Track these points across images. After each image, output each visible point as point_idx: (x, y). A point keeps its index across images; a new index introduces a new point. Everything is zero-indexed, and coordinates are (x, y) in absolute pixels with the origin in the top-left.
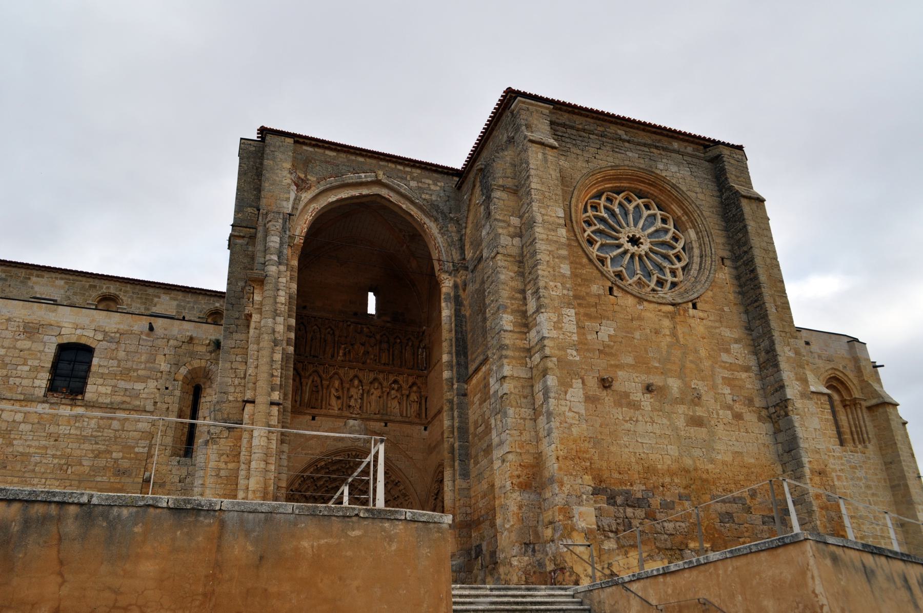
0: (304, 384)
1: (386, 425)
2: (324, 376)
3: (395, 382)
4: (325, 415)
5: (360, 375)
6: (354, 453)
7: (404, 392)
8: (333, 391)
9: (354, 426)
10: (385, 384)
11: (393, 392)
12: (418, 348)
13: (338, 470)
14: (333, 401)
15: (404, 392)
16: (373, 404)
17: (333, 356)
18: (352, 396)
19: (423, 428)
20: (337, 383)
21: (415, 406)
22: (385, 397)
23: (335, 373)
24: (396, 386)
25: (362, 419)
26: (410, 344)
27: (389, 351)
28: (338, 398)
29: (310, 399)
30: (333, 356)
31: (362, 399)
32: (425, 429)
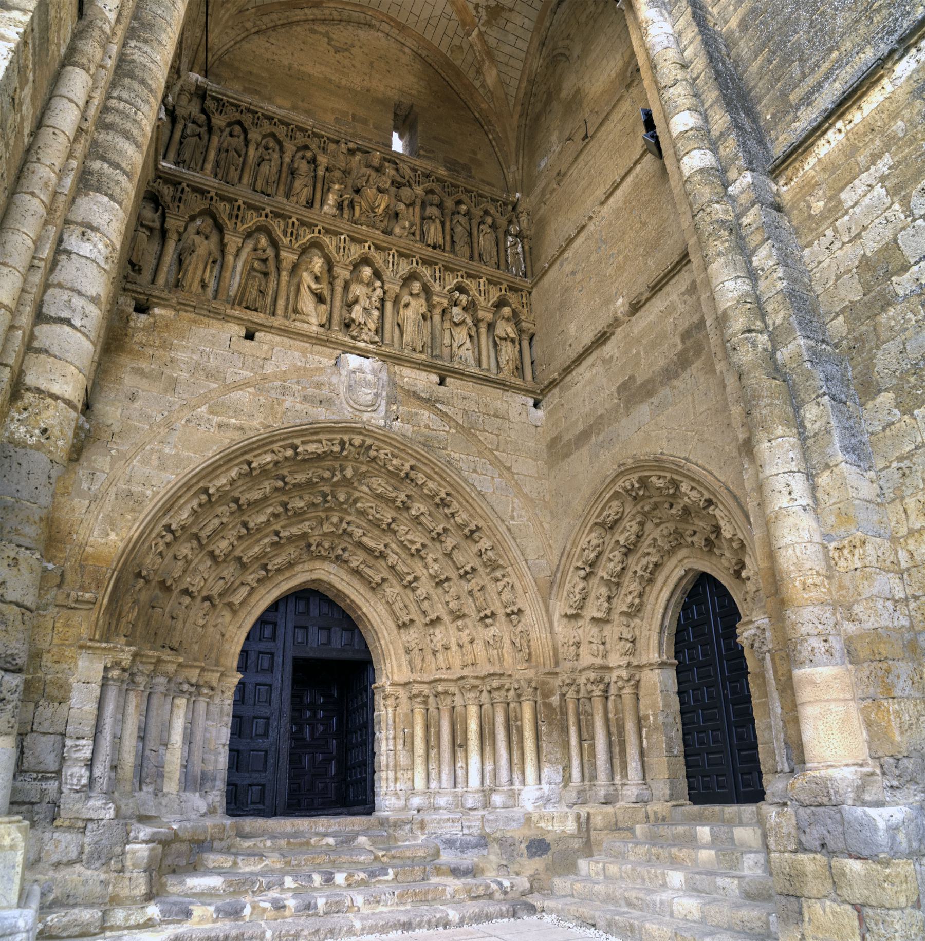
0: (231, 249)
1: (442, 382)
2: (286, 241)
3: (461, 289)
4: (284, 332)
5: (378, 258)
6: (357, 440)
7: (481, 314)
8: (307, 278)
9: (361, 370)
10: (436, 287)
11: (456, 310)
12: (507, 233)
13: (310, 484)
14: (307, 303)
15: (481, 314)
16: (409, 328)
17: (310, 204)
18: (356, 301)
19: (531, 402)
20: (318, 264)
21: (508, 352)
22: (437, 318)
23: (316, 244)
24: (464, 299)
25: (385, 358)
27: (443, 224)
28: (320, 299)
29: (243, 289)
30: (310, 204)
31: (382, 309)
32: (536, 405)
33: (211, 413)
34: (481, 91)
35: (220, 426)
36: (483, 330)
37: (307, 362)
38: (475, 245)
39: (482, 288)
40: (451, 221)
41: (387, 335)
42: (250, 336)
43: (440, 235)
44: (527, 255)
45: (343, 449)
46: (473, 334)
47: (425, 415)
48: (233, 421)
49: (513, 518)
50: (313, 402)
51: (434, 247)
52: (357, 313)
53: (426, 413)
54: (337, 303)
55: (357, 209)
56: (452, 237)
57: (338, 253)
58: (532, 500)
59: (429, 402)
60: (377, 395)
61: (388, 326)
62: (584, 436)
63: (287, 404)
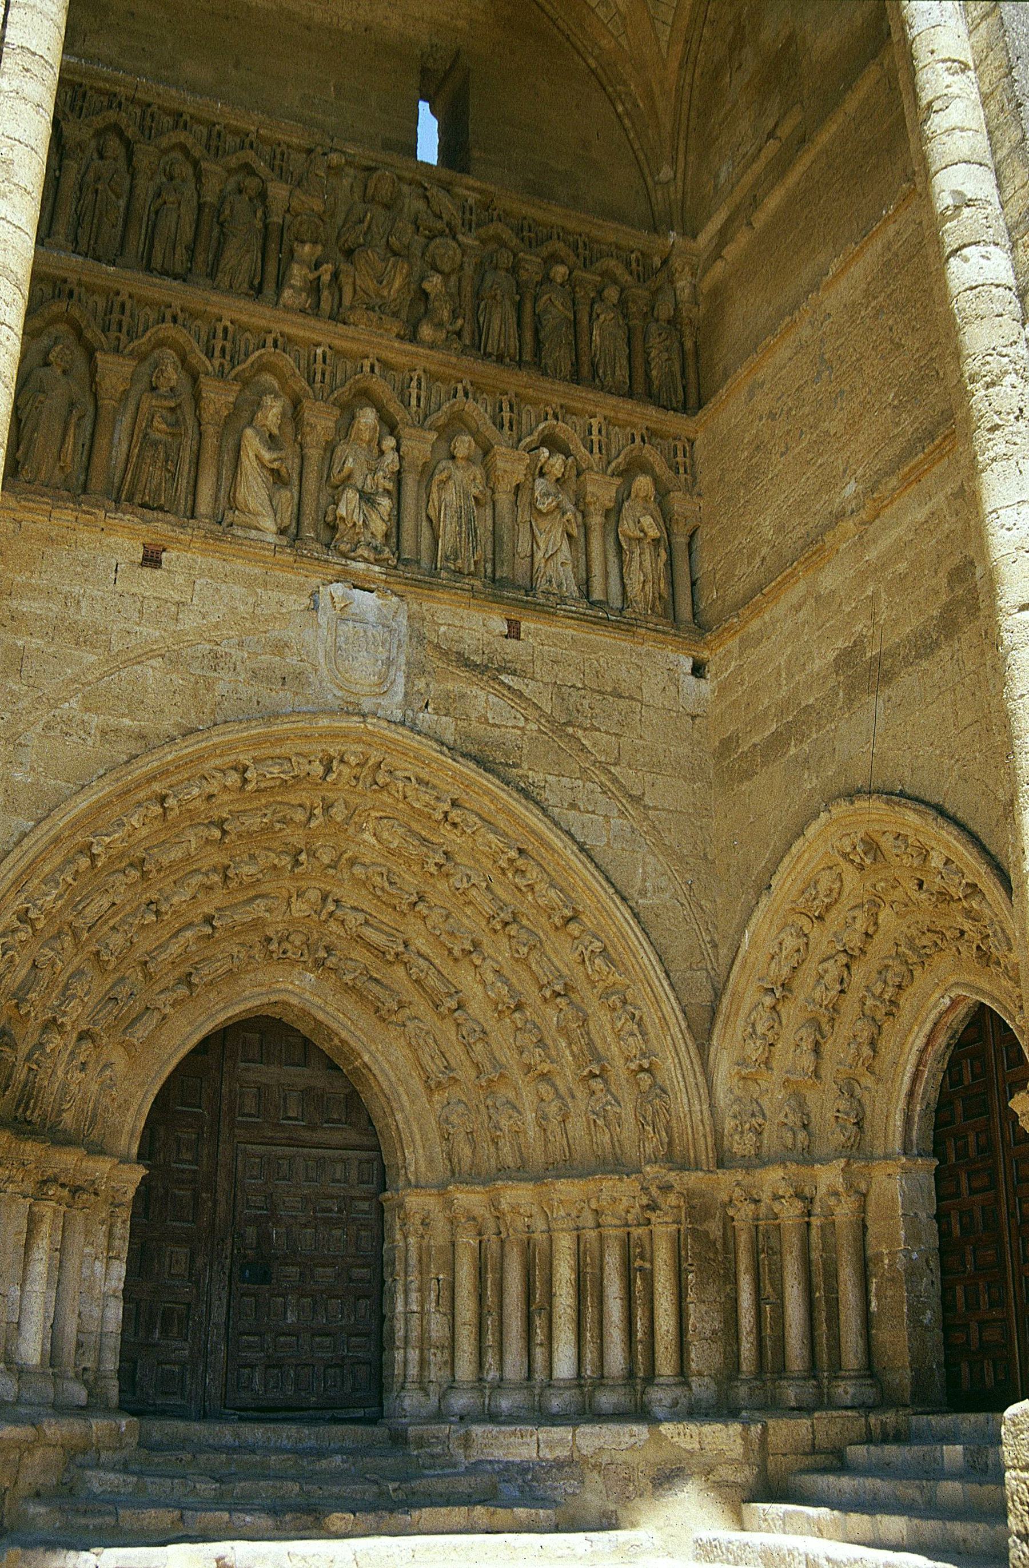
1: (514, 631)
3: (552, 442)
11: (540, 485)
16: (448, 529)
26: (612, 294)
31: (397, 496)
32: (698, 670)
33: (88, 710)
34: (601, 12)
35: (104, 733)
36: (596, 520)
37: (256, 605)
38: (583, 345)
39: (595, 437)
40: (536, 299)
41: (408, 542)
42: (152, 559)
43: (513, 330)
44: (690, 361)
45: (328, 770)
46: (575, 532)
47: (482, 699)
48: (127, 721)
49: (643, 893)
50: (269, 680)
51: (500, 359)
52: (349, 505)
53: (482, 694)
54: (311, 482)
55: (348, 291)
56: (536, 332)
57: (311, 381)
58: (681, 859)
59: (486, 669)
60: (389, 663)
61: (408, 524)
62: (777, 742)
63: (221, 688)
